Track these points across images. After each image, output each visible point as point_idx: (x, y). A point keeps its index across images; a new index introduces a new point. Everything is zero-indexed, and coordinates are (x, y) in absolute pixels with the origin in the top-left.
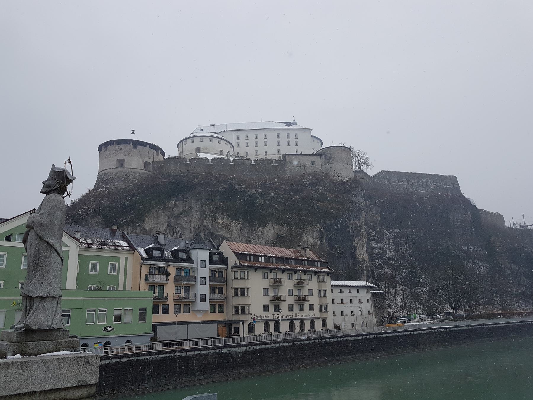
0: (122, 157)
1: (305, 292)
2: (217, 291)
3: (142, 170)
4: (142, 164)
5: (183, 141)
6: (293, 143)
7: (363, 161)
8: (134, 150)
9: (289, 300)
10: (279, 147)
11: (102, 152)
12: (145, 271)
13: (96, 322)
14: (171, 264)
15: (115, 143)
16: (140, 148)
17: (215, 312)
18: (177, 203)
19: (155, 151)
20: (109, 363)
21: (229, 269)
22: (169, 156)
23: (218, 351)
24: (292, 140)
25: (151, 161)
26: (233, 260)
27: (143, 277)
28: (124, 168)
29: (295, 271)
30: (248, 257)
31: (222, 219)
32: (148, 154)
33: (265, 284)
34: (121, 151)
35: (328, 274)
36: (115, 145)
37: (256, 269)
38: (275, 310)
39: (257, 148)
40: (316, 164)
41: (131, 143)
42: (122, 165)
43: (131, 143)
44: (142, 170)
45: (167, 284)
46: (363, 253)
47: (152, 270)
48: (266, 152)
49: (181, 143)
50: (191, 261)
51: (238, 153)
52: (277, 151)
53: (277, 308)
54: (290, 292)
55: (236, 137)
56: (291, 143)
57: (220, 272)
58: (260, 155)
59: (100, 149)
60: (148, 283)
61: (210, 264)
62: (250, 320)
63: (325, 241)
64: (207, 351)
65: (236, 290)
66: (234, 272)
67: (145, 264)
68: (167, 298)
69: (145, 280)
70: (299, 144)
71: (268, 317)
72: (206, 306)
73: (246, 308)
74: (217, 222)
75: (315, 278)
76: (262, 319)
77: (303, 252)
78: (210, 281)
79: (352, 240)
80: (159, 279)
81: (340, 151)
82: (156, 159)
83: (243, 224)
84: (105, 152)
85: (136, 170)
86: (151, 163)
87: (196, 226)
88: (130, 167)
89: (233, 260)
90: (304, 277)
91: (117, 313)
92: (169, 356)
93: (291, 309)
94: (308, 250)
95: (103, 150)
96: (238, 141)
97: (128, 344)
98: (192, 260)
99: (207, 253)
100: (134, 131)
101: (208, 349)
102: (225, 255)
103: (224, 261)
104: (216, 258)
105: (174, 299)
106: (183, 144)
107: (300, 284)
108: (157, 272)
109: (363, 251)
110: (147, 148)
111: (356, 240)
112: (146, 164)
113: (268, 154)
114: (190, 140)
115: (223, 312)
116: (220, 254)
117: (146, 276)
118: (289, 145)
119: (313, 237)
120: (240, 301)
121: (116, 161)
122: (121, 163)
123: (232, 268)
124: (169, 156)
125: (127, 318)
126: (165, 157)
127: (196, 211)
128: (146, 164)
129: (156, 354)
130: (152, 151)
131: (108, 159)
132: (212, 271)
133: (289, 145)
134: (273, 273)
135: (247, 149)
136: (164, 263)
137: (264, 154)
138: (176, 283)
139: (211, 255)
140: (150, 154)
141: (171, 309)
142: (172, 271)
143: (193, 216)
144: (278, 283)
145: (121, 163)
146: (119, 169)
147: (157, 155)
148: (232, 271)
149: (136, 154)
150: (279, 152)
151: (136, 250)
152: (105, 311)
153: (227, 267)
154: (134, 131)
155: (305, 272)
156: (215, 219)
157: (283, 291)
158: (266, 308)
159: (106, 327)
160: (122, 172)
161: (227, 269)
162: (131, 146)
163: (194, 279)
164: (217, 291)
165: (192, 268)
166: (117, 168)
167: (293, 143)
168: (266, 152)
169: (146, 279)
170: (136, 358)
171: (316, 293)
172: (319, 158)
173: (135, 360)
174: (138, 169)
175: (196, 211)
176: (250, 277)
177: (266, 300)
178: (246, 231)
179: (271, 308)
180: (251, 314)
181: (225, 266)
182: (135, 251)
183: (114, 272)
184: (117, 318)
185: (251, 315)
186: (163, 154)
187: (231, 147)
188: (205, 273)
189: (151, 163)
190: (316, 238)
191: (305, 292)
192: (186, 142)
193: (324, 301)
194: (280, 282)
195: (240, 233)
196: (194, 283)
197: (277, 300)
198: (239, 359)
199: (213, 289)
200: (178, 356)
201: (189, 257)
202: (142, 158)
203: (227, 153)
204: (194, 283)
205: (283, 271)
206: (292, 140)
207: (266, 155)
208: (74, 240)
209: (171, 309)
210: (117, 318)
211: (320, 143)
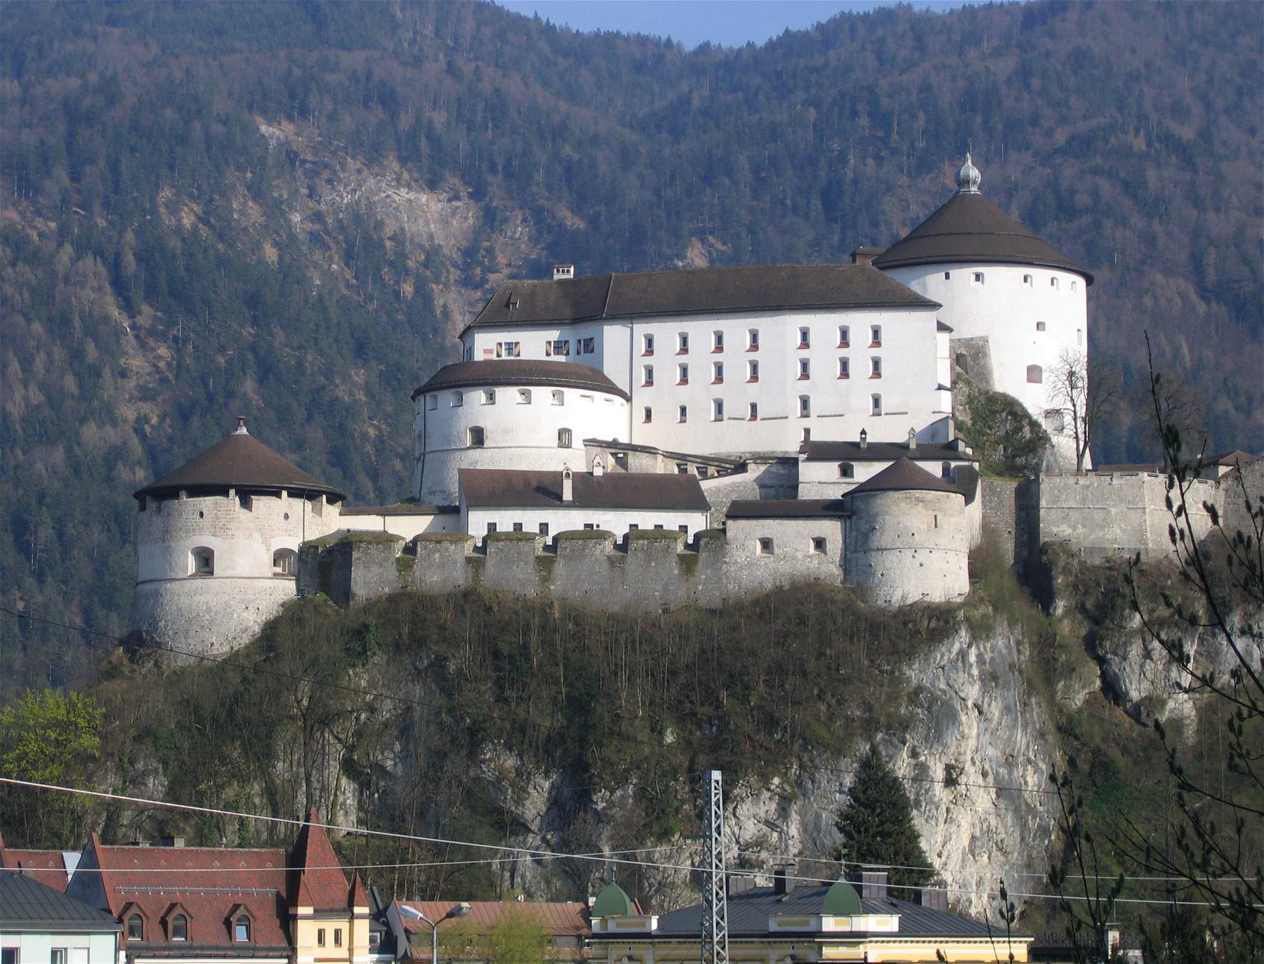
10: (804, 387)
16: (260, 503)
19: (309, 505)
39: (718, 391)
41: (232, 492)
43: (232, 492)
48: (754, 407)
55: (641, 345)
58: (729, 418)
81: (902, 505)
88: (229, 573)
95: (148, 511)
96: (649, 360)
109: (945, 854)
118: (845, 374)
133: (845, 374)
147: (318, 512)
162: (234, 500)
168: (754, 407)
202: (266, 541)
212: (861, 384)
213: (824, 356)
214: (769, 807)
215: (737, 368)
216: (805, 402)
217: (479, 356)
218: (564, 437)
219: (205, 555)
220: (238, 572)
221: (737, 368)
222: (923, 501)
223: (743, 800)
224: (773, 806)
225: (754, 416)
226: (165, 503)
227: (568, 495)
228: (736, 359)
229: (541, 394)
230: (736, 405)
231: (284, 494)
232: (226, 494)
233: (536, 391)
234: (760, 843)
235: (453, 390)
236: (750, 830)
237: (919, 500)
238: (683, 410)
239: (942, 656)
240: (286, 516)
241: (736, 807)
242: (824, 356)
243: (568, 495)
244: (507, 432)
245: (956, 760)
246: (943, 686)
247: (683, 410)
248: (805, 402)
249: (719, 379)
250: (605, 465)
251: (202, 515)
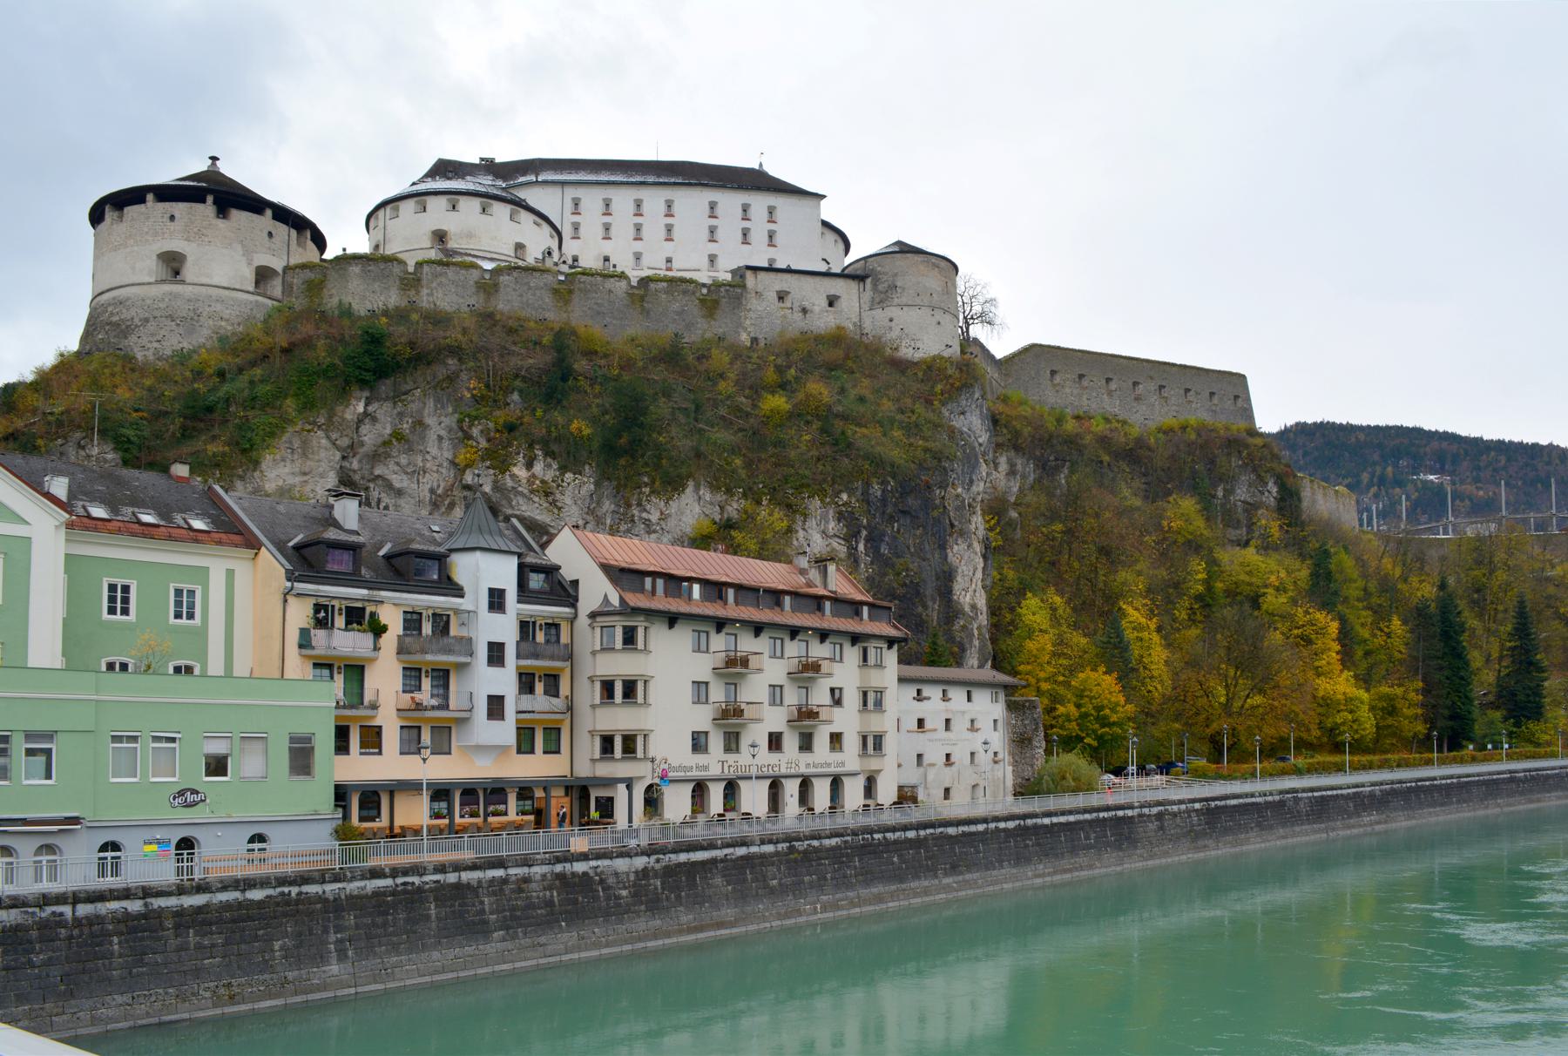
1: (820, 696)
2: (539, 687)
3: (248, 292)
4: (249, 276)
5: (388, 208)
7: (977, 309)
8: (221, 223)
9: (776, 719)
11: (102, 226)
12: (300, 614)
13: (145, 775)
14: (390, 598)
15: (150, 197)
16: (239, 217)
17: (532, 751)
18: (370, 408)
19: (294, 233)
20: (207, 905)
21: (583, 620)
22: (344, 250)
23: (558, 868)
25: (278, 264)
26: (596, 590)
27: (293, 638)
28: (183, 282)
29: (794, 632)
30: (648, 581)
31: (529, 465)
32: (267, 238)
33: (703, 667)
34: (172, 226)
35: (891, 642)
37: (672, 620)
38: (728, 749)
40: (843, 304)
41: (210, 199)
42: (177, 273)
43: (210, 199)
44: (248, 292)
45: (372, 660)
46: (973, 586)
47: (322, 617)
48: (669, 260)
49: (381, 213)
50: (458, 591)
51: (575, 259)
53: (732, 742)
54: (776, 691)
55: (569, 206)
56: (753, 236)
57: (553, 627)
59: (96, 215)
60: (309, 657)
61: (518, 602)
62: (650, 777)
63: (861, 547)
64: (525, 870)
65: (608, 687)
66: (602, 627)
67: (299, 595)
68: (374, 706)
69: (301, 646)
70: (778, 239)
71: (706, 768)
72: (505, 732)
73: (640, 741)
74: (513, 476)
75: (852, 654)
76: (688, 774)
77: (814, 575)
78: (519, 656)
79: (943, 547)
80: (346, 642)
82: (293, 262)
83: (597, 484)
84: (115, 226)
85: (227, 292)
86: (279, 269)
87: (439, 486)
88: (205, 280)
89: (596, 590)
90: (819, 651)
91: (217, 748)
92: (405, 884)
93: (775, 742)
94: (832, 568)
96: (576, 218)
97: (256, 846)
98: (456, 584)
99: (512, 564)
100: (218, 159)
101: (526, 862)
102: (568, 574)
103: (564, 592)
104: (536, 581)
105: (398, 710)
106: (388, 217)
107: (808, 671)
108: (340, 621)
109: (974, 580)
110: (266, 220)
111: (956, 547)
112: (263, 275)
114: (410, 204)
115: (558, 752)
116: (551, 571)
117: (304, 633)
119: (824, 533)
120: (619, 719)
121: (155, 258)
122: (173, 264)
123: (593, 615)
124: (344, 250)
125: (246, 765)
126: (329, 254)
127: (439, 436)
128: (263, 275)
129: (363, 878)
130: (282, 230)
131: (128, 250)
132: (526, 628)
134: (727, 634)
135: (608, 248)
136: (365, 592)
138: (402, 657)
139: (523, 570)
140: (273, 240)
141: (391, 738)
142: (392, 618)
143: (428, 453)
144: (735, 667)
145: (173, 264)
146: (167, 288)
148: (595, 624)
149: (225, 237)
150: (712, 259)
151: (263, 548)
152: (173, 740)
153: (573, 611)
154: (218, 159)
155: (823, 635)
156: (503, 466)
157: (754, 690)
158: (699, 743)
159: (181, 793)
160: (176, 296)
161: (572, 620)
163: (467, 645)
164: (539, 687)
165: (457, 611)
166: (157, 282)
168: (669, 260)
169: (305, 642)
170: (294, 890)
171: (851, 699)
173: (293, 894)
174: (234, 289)
175: (439, 436)
176: (651, 647)
177: (702, 718)
178: (608, 506)
179: (716, 742)
180: (653, 760)
181: (567, 610)
182: (259, 549)
183: (191, 616)
184: (217, 766)
185: (653, 761)
186: (320, 241)
187: (552, 237)
188: (504, 628)
189: (279, 269)
190: (835, 536)
191: (820, 696)
192: (397, 209)
193: (876, 723)
194: (745, 662)
195: (587, 513)
196: (468, 660)
197: (731, 720)
198: (624, 893)
199: (526, 683)
200: (435, 882)
201: (449, 578)
202: (248, 253)
203: (543, 253)
204: (468, 660)
205: (758, 629)
207: (669, 269)
208: (49, 503)
209: (391, 738)
210: (217, 766)
211: (841, 246)
219: (175, 265)
220: (215, 281)
226: (126, 210)
229: (501, 210)
231: (269, 213)
232: (203, 201)
235: (416, 199)
240: (270, 234)
244: (470, 235)
249: (638, 238)
251: (172, 218)
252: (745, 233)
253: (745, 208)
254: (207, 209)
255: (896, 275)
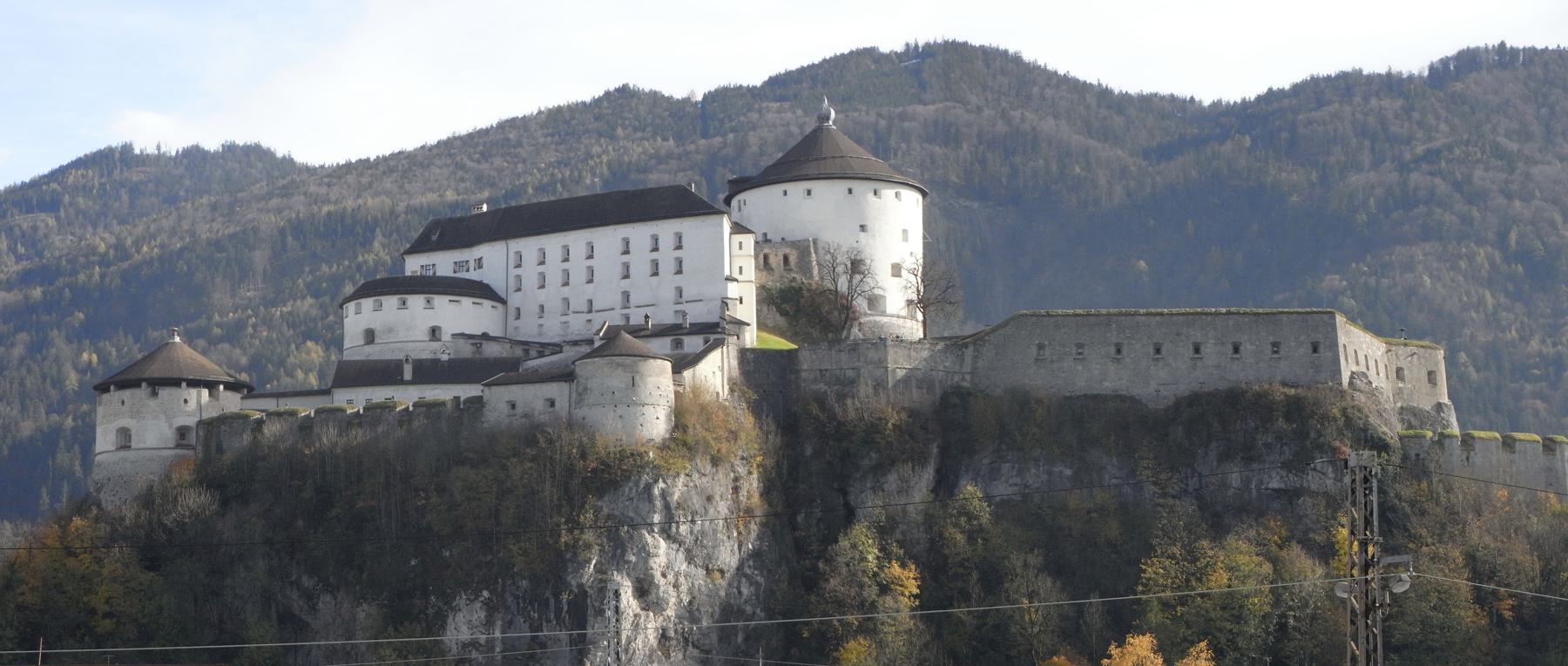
0: (126, 422)
3: (170, 448)
6: (667, 267)
8: (152, 403)
16: (165, 393)
24: (667, 256)
36: (112, 393)
41: (144, 384)
44: (170, 448)
52: (617, 299)
58: (574, 312)
81: (606, 369)
85: (155, 452)
88: (142, 446)
96: (518, 271)
113: (596, 306)
119: (471, 626)
137: (586, 310)
146: (123, 454)
167: (667, 267)
168: (590, 302)
172: (564, 386)
174: (160, 449)
206: (667, 256)
207: (590, 311)
212: (667, 280)
213: (640, 261)
214: (479, 614)
215: (578, 276)
216: (626, 296)
217: (408, 273)
218: (434, 332)
220: (149, 444)
221: (578, 276)
222: (622, 366)
223: (460, 610)
224: (483, 614)
225: (590, 311)
227: (408, 375)
228: (578, 266)
229: (416, 301)
230: (578, 303)
231: (184, 384)
232: (139, 386)
233: (384, 299)
234: (474, 644)
236: (465, 635)
237: (618, 365)
238: (542, 307)
239: (631, 489)
241: (455, 615)
242: (640, 261)
243: (408, 375)
244: (390, 330)
245: (644, 575)
246: (631, 514)
247: (542, 307)
248: (626, 296)
250: (466, 350)
251: (123, 403)
252: (655, 264)
253: (655, 239)
254: (143, 392)
255: (587, 379)
